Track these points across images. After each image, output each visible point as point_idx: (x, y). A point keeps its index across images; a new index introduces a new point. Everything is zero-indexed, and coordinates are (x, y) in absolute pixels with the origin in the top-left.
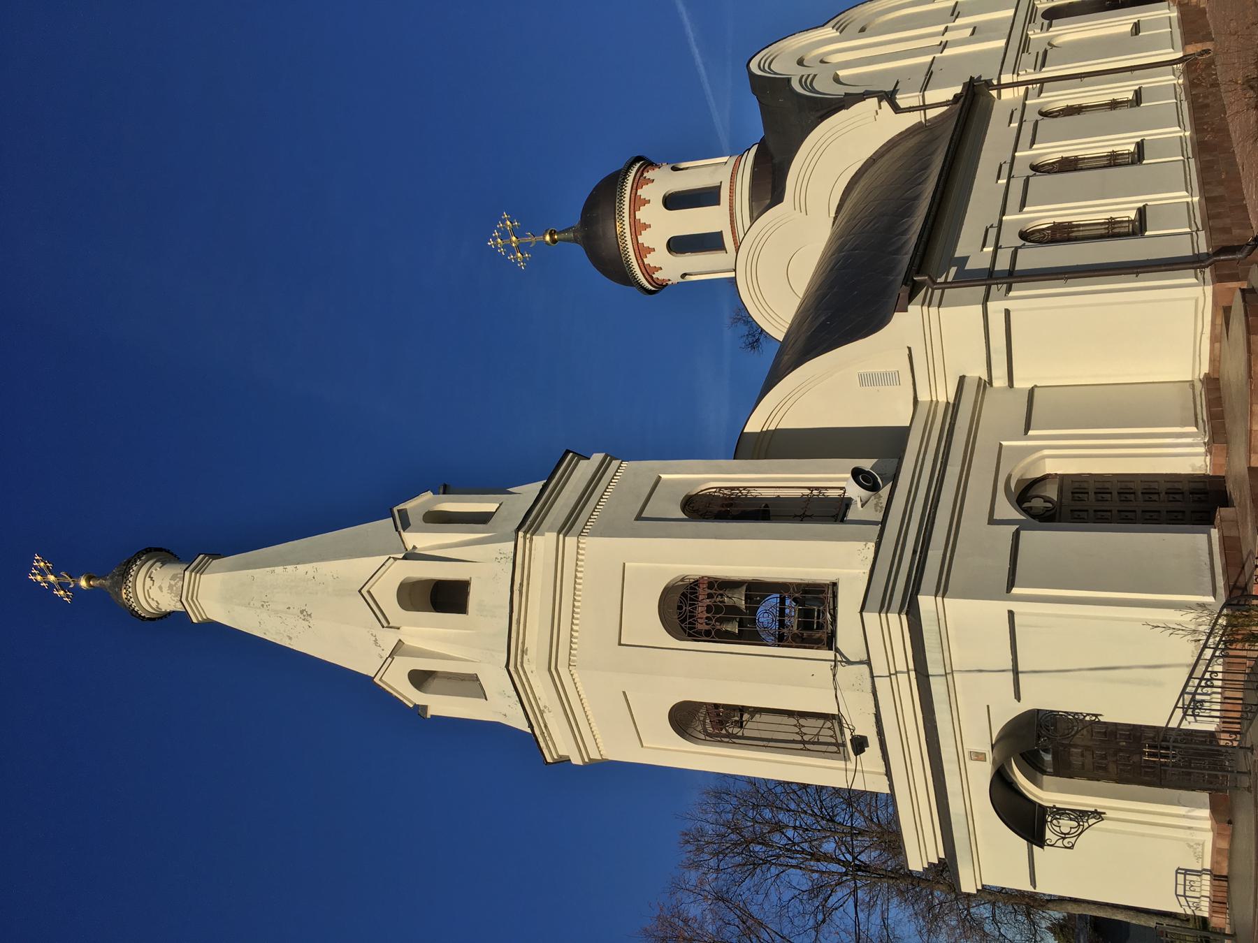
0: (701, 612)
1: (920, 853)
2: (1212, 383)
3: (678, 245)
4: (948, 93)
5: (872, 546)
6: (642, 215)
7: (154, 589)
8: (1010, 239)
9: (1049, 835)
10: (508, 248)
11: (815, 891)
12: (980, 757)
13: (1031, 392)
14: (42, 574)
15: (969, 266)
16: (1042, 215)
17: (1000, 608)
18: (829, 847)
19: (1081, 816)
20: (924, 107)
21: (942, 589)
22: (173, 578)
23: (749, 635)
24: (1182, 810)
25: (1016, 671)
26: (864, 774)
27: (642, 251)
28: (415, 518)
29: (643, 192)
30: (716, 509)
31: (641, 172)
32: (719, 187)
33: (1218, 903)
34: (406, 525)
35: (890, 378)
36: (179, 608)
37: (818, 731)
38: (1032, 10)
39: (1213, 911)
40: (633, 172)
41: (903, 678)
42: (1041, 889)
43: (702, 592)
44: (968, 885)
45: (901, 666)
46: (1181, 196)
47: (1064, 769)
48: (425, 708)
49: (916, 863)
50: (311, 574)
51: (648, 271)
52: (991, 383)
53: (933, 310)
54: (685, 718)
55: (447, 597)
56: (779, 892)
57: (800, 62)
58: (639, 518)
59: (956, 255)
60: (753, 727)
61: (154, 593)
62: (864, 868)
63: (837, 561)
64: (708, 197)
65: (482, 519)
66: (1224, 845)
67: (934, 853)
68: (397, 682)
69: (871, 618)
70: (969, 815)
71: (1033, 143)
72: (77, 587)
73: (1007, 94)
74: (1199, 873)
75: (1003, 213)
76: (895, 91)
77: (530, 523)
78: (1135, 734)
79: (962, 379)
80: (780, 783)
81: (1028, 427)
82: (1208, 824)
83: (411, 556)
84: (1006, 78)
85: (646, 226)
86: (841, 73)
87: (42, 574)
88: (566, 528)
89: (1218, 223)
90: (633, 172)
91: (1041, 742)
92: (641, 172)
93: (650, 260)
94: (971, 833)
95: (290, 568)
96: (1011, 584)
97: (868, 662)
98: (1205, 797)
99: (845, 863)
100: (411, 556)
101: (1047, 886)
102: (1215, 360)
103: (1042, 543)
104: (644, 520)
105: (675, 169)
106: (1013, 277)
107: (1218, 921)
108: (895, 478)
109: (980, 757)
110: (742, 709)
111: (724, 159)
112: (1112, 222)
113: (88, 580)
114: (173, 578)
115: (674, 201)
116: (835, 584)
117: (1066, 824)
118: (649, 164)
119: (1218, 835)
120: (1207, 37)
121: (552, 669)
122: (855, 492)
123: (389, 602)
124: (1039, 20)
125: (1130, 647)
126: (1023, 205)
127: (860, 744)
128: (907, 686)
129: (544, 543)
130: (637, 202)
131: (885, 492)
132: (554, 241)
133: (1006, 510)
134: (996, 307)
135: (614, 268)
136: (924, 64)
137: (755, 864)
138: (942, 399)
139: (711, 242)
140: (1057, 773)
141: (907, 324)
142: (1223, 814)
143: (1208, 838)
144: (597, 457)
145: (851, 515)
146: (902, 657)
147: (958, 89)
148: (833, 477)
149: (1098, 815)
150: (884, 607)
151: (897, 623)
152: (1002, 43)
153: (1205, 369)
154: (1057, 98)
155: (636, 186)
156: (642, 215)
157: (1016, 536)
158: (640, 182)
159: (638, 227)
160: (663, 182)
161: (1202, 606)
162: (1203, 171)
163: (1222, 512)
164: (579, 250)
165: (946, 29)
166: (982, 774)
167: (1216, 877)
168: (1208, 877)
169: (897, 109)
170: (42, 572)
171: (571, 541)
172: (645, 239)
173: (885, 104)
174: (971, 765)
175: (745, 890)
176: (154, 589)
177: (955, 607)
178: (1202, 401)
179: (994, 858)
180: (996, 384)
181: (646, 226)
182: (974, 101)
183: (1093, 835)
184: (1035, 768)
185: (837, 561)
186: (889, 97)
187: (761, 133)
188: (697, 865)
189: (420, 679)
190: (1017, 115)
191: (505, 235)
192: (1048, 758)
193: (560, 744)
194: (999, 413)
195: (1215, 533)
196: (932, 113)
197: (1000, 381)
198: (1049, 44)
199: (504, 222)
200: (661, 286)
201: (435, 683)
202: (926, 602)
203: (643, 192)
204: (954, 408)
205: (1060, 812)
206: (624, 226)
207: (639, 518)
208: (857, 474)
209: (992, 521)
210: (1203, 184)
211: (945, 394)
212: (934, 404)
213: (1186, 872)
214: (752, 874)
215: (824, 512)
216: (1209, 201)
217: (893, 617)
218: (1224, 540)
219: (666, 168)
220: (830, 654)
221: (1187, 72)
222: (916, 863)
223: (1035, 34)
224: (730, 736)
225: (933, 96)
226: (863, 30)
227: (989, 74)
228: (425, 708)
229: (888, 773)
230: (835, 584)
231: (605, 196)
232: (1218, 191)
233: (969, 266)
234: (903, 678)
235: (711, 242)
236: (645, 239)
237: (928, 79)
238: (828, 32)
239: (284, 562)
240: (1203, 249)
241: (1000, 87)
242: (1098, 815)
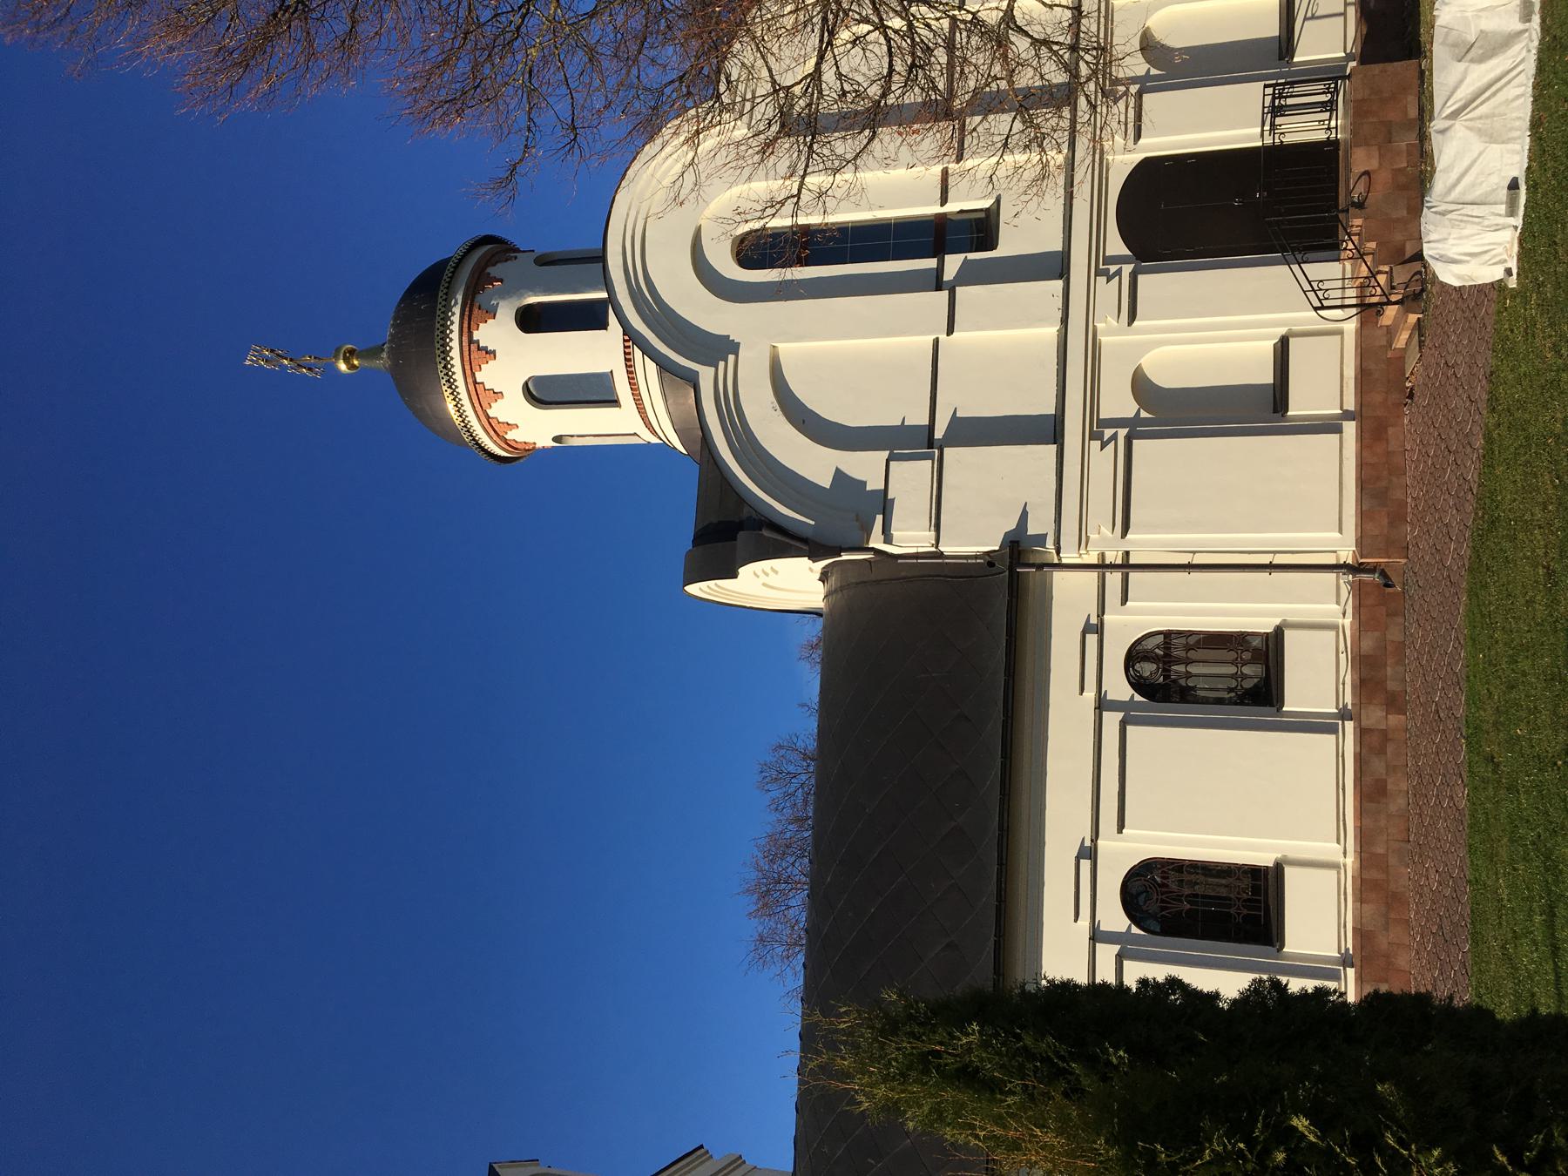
29: (488, 375)
32: (606, 380)
40: (455, 344)
71: (1121, 826)
76: (884, 503)
84: (1068, 557)
86: (781, 346)
90: (455, 344)
115: (543, 393)
120: (1391, 545)
124: (1116, 245)
155: (470, 371)
203: (488, 375)
221: (1359, 591)
223: (1112, 332)
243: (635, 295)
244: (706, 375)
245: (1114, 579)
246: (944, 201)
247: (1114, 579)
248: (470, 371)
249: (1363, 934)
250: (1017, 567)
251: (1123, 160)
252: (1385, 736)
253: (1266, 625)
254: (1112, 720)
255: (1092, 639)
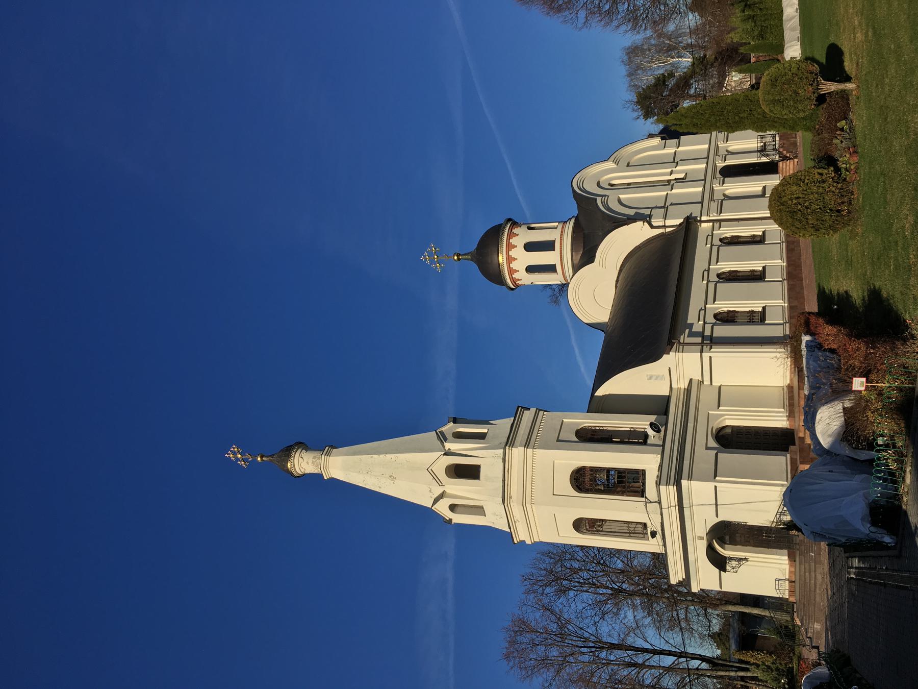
0: (587, 479)
1: (676, 575)
2: (790, 388)
3: (531, 269)
4: (678, 222)
5: (659, 456)
6: (512, 253)
7: (303, 463)
8: (710, 319)
9: (728, 567)
10: (432, 261)
11: (597, 603)
12: (702, 538)
13: (720, 387)
14: (234, 454)
15: (694, 330)
16: (723, 306)
17: (713, 484)
18: (604, 580)
19: (740, 560)
20: (664, 227)
21: (690, 478)
22: (314, 458)
23: (609, 489)
24: (778, 557)
25: (716, 505)
26: (652, 546)
27: (512, 271)
28: (449, 436)
29: (513, 241)
30: (589, 436)
31: (511, 229)
32: (554, 241)
33: (792, 592)
34: (442, 438)
35: (659, 378)
36: (316, 472)
37: (639, 530)
38: (715, 166)
39: (790, 596)
41: (673, 508)
42: (724, 589)
43: (588, 473)
44: (695, 589)
45: (673, 504)
46: (780, 302)
47: (734, 542)
48: (451, 520)
49: (673, 581)
50: (394, 459)
51: (514, 281)
52: (703, 382)
53: (680, 354)
54: (579, 525)
55: (469, 472)
56: (577, 605)
57: (598, 184)
58: (558, 440)
59: (689, 322)
60: (605, 528)
61: (304, 465)
62: (620, 591)
63: (647, 462)
64: (548, 246)
65: (481, 437)
66: (793, 569)
67: (681, 576)
68: (442, 508)
69: (663, 488)
70: (696, 561)
71: (717, 262)
72: (255, 460)
73: (704, 225)
74: (784, 580)
75: (706, 303)
76: (650, 216)
77: (510, 442)
78: (760, 529)
79: (691, 380)
80: (578, 546)
81: (719, 406)
82: (787, 562)
83: (448, 453)
84: (704, 218)
85: (515, 259)
86: (621, 196)
87: (234, 454)
88: (527, 445)
89: (794, 321)
91: (724, 533)
92: (511, 229)
93: (515, 276)
94: (697, 568)
95: (382, 456)
96: (715, 476)
97: (660, 503)
98: (786, 552)
99: (612, 589)
100: (448, 453)
101: (726, 588)
102: (791, 380)
103: (728, 458)
104: (560, 442)
105: (530, 228)
106: (712, 341)
107: (792, 599)
108: (666, 424)
109: (702, 538)
110: (603, 520)
111: (556, 224)
112: (754, 236)
113: (261, 457)
114: (314, 458)
115: (530, 247)
116: (644, 471)
117: (734, 563)
118: (515, 224)
119: (791, 566)
121: (524, 504)
122: (650, 432)
123: (442, 475)
124: (718, 175)
125: (758, 497)
126: (715, 300)
127: (654, 534)
128: (675, 512)
129: (517, 453)
130: (510, 247)
131: (663, 429)
132: (459, 259)
133: (712, 443)
134: (706, 356)
135: (495, 276)
136: (661, 196)
137: (563, 591)
138: (682, 387)
139: (551, 269)
140: (730, 544)
141: (668, 360)
142: (792, 557)
143: (787, 567)
144: (533, 410)
145: (649, 442)
146: (674, 500)
147: (682, 220)
148: (642, 423)
149: (746, 559)
150: (668, 483)
151: (672, 489)
152: (700, 189)
153: (788, 382)
154: (729, 231)
155: (509, 238)
156: (512, 253)
157: (716, 455)
158: (511, 235)
159: (510, 259)
160: (523, 236)
161: (782, 485)
162: (789, 290)
163: (792, 448)
164: (474, 267)
165: (671, 173)
166: (702, 546)
167: (790, 582)
168: (787, 582)
169: (652, 227)
170: (234, 454)
171: (530, 451)
172: (514, 265)
173: (646, 224)
174: (699, 542)
175: (559, 604)
176: (303, 463)
177: (695, 485)
178: (786, 396)
179: (706, 578)
180: (705, 383)
181: (515, 259)
182: (690, 224)
183: (744, 568)
184: (722, 543)
185: (647, 462)
186: (647, 219)
187: (576, 213)
188: (535, 592)
189: (453, 508)
190: (710, 238)
191: (431, 255)
192: (727, 538)
193: (522, 535)
194: (708, 397)
195: (788, 456)
196: (668, 230)
197: (707, 381)
198: (724, 195)
199: (431, 248)
200: (518, 286)
201: (458, 509)
202: (684, 483)
204: (688, 391)
205: (731, 559)
206: (502, 259)
207: (558, 440)
208: (651, 425)
209: (707, 448)
210: (789, 298)
211: (684, 385)
212: (679, 389)
213: (779, 580)
214: (559, 598)
215: (638, 439)
216: (791, 308)
217: (671, 487)
218: (791, 459)
219: (524, 228)
220: (643, 499)
222: (673, 581)
223: (717, 187)
224: (598, 531)
225: (668, 223)
226: (628, 165)
227: (695, 210)
228: (451, 520)
229: (665, 545)
230: (644, 471)
231: (492, 239)
232: (795, 303)
233: (694, 330)
234: (673, 508)
235: (551, 269)
236: (514, 265)
237: (665, 208)
238: (610, 165)
239: (379, 453)
240: (788, 333)
241: (701, 221)
242: (746, 559)
243: (580, 189)
244: (599, 199)
245: (716, 225)
246: (671, 173)
247: (716, 225)
248: (509, 238)
249: (788, 273)
250: (690, 224)
251: (720, 164)
252: (793, 242)
253: (761, 233)
254: (715, 249)
255: (710, 238)
